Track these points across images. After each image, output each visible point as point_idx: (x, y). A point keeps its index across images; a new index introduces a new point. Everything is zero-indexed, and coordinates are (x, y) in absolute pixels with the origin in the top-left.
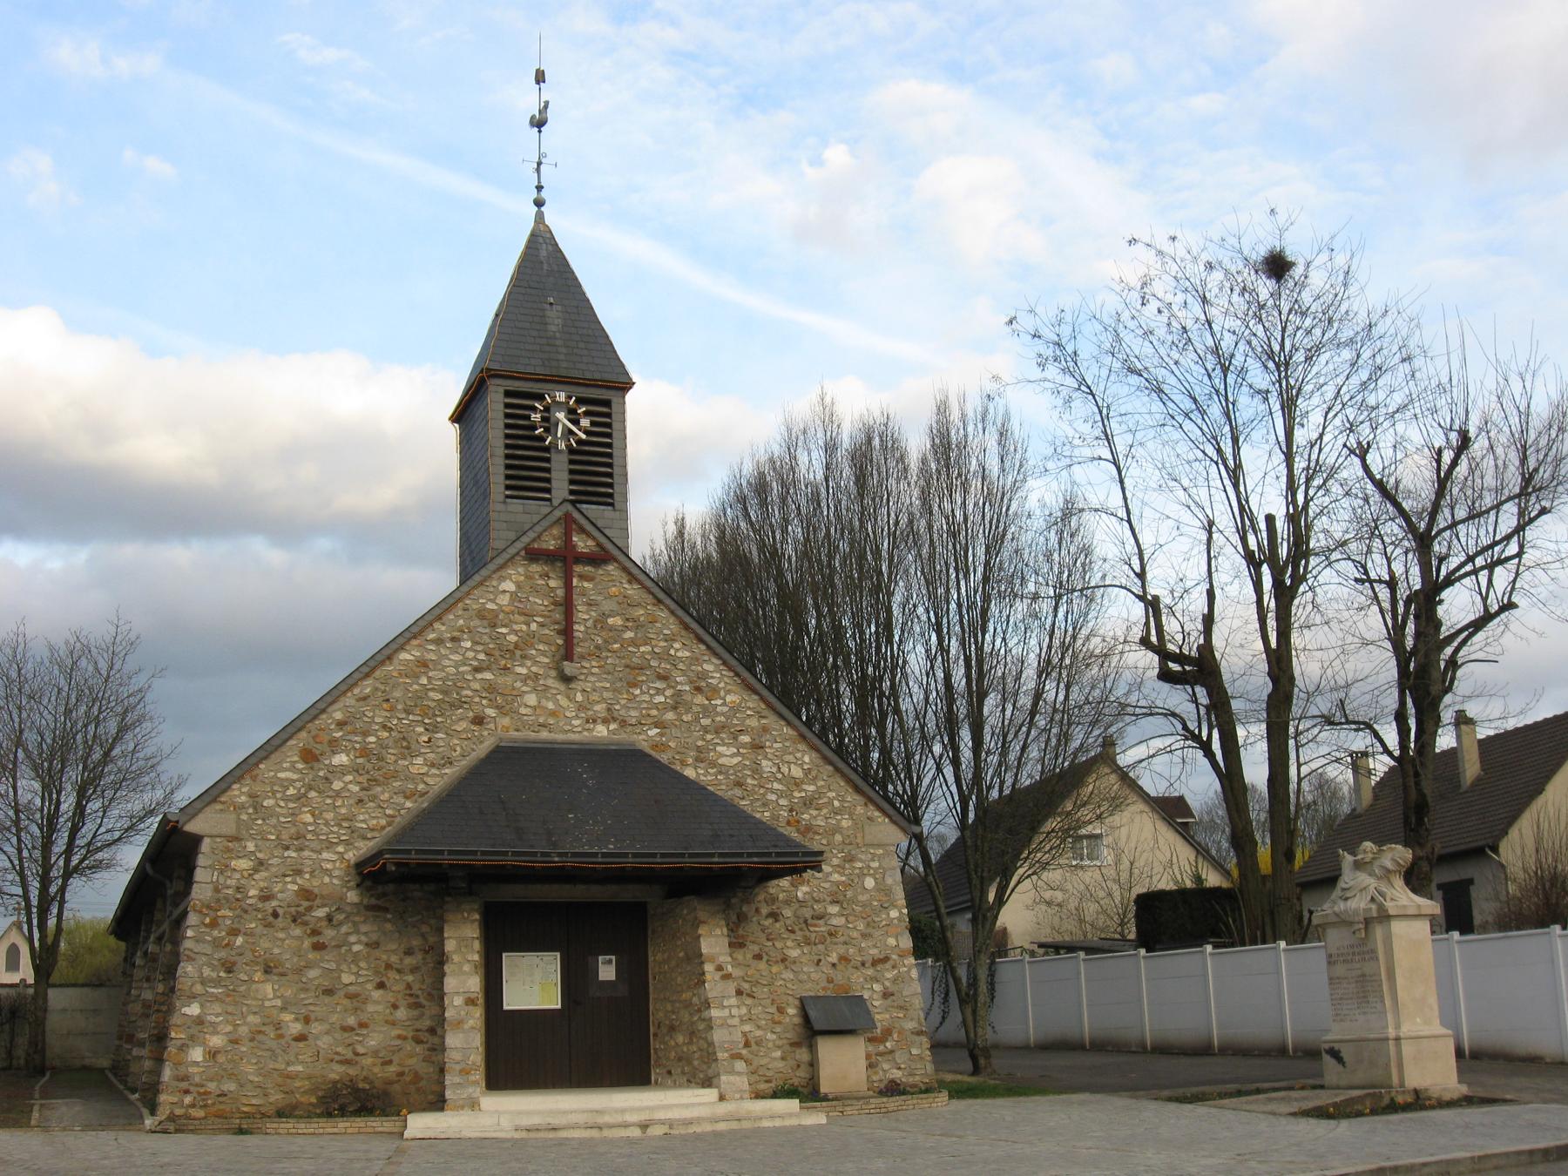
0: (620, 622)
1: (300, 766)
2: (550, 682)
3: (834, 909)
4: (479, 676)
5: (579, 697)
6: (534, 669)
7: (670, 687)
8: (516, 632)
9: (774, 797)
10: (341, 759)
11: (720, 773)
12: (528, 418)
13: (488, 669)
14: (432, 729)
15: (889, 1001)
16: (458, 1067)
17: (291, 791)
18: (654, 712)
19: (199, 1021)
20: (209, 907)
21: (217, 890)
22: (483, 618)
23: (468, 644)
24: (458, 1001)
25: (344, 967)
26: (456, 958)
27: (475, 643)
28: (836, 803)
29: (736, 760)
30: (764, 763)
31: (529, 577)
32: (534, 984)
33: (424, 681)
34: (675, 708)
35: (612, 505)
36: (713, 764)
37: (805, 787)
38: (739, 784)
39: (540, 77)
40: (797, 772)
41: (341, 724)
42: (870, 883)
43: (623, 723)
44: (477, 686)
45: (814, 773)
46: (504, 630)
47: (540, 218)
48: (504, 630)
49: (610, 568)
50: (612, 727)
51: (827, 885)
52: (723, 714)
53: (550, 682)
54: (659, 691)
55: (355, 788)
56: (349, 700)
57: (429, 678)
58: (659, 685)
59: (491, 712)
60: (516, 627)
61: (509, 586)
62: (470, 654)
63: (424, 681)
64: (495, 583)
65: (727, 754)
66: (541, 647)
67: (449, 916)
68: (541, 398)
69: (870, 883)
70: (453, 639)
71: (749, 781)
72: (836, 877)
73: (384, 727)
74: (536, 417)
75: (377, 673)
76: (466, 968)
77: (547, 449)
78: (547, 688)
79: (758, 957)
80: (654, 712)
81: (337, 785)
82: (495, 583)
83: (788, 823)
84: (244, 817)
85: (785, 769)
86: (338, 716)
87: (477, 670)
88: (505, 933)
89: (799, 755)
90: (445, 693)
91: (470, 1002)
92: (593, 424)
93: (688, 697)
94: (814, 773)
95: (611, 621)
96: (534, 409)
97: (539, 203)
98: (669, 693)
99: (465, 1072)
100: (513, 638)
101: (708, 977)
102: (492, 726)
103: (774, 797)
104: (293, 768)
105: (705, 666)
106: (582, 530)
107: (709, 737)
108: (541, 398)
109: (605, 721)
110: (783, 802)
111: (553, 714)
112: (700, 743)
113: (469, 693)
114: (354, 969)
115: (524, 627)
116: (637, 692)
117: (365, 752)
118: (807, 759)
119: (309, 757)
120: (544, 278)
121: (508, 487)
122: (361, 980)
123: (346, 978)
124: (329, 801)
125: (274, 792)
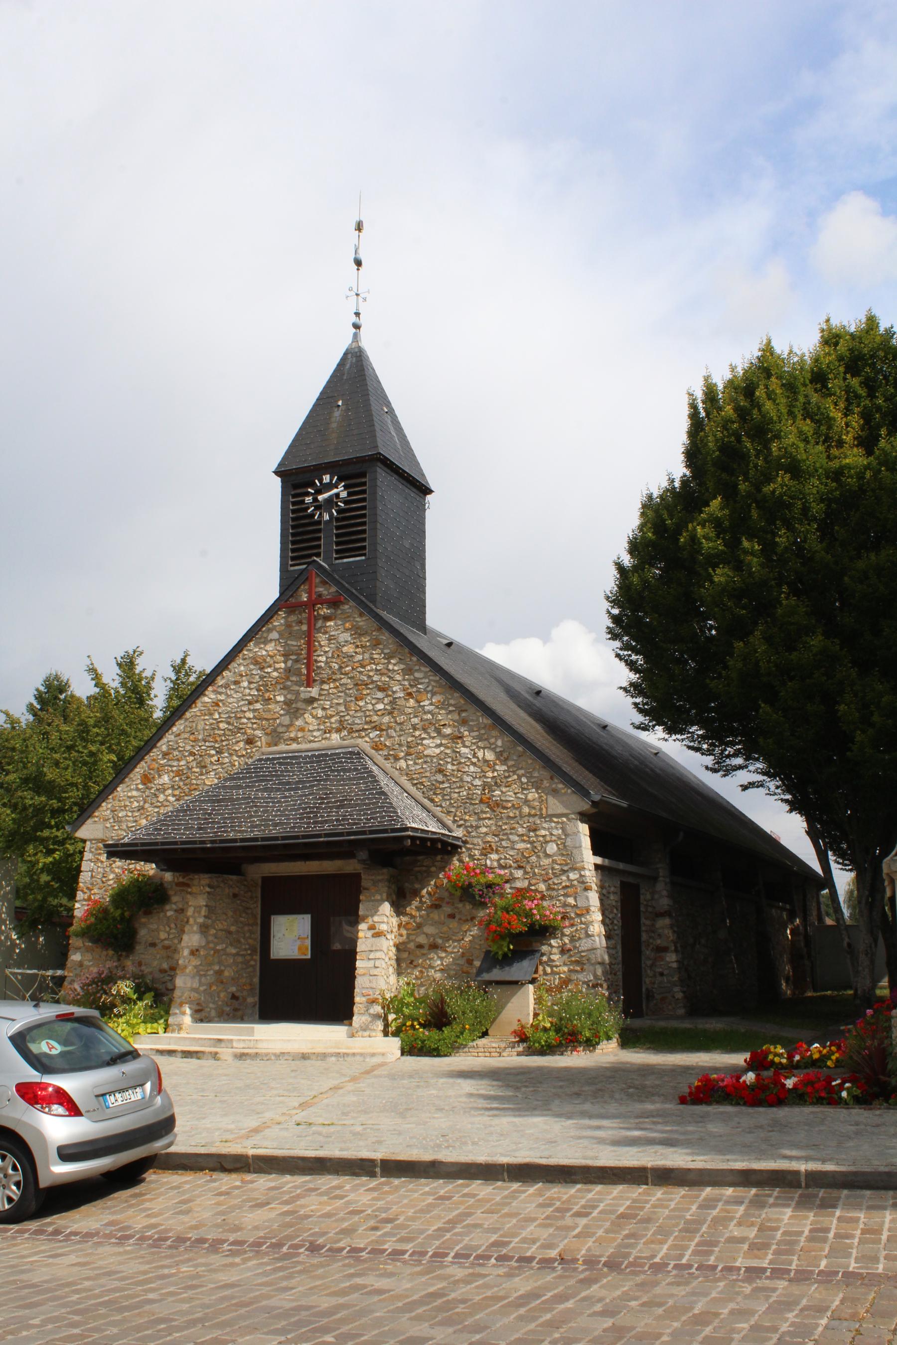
0: (352, 650)
1: (140, 786)
2: (300, 705)
3: (519, 874)
4: (251, 707)
5: (320, 713)
6: (289, 696)
7: (387, 696)
8: (276, 670)
9: (469, 779)
10: (166, 779)
11: (426, 762)
12: (303, 502)
13: (257, 701)
14: (219, 752)
15: (565, 957)
16: (179, 1001)
17: (136, 804)
18: (375, 718)
19: (81, 964)
20: (88, 888)
21: (92, 877)
22: (256, 663)
23: (245, 684)
24: (186, 952)
25: (161, 927)
26: (191, 921)
27: (250, 683)
28: (524, 780)
29: (437, 751)
30: (464, 750)
31: (288, 626)
32: (291, 936)
33: (217, 716)
34: (390, 713)
35: (364, 555)
36: (419, 755)
37: (497, 767)
38: (440, 771)
39: (359, 227)
40: (490, 756)
41: (165, 755)
42: (552, 848)
43: (351, 731)
44: (250, 715)
45: (505, 755)
46: (269, 670)
47: (356, 337)
48: (269, 670)
49: (346, 607)
50: (343, 734)
51: (511, 853)
52: (429, 712)
53: (300, 705)
54: (379, 700)
55: (172, 799)
56: (169, 737)
57: (219, 713)
58: (380, 695)
59: (258, 733)
60: (277, 666)
61: (274, 635)
62: (247, 691)
63: (217, 716)
64: (265, 635)
65: (432, 746)
66: (294, 679)
67: (194, 889)
68: (313, 485)
69: (552, 848)
70: (236, 683)
71: (449, 766)
72: (521, 846)
73: (192, 754)
74: (309, 499)
75: (188, 715)
76: (195, 928)
77: (319, 523)
78: (298, 709)
79: (452, 916)
80: (375, 718)
81: (162, 797)
82: (265, 635)
83: (481, 801)
84: (108, 825)
85: (480, 754)
86: (164, 748)
87: (250, 703)
88: (280, 898)
89: (493, 740)
90: (228, 723)
91: (193, 953)
92: (349, 494)
93: (401, 702)
94: (505, 755)
95: (345, 649)
96: (308, 494)
97: (357, 326)
98: (386, 701)
99: (181, 1005)
100: (275, 674)
101: (361, 934)
102: (259, 744)
103: (469, 779)
104: (138, 789)
105: (417, 675)
106: (324, 583)
107: (417, 733)
108: (313, 485)
109: (338, 731)
110: (478, 782)
111: (302, 729)
112: (410, 739)
113: (245, 721)
114: (168, 929)
115: (283, 665)
116: (361, 703)
117: (179, 773)
118: (499, 743)
119: (147, 779)
120: (353, 383)
121: (293, 559)
122: (171, 936)
123: (163, 935)
124: (156, 810)
125: (125, 806)
